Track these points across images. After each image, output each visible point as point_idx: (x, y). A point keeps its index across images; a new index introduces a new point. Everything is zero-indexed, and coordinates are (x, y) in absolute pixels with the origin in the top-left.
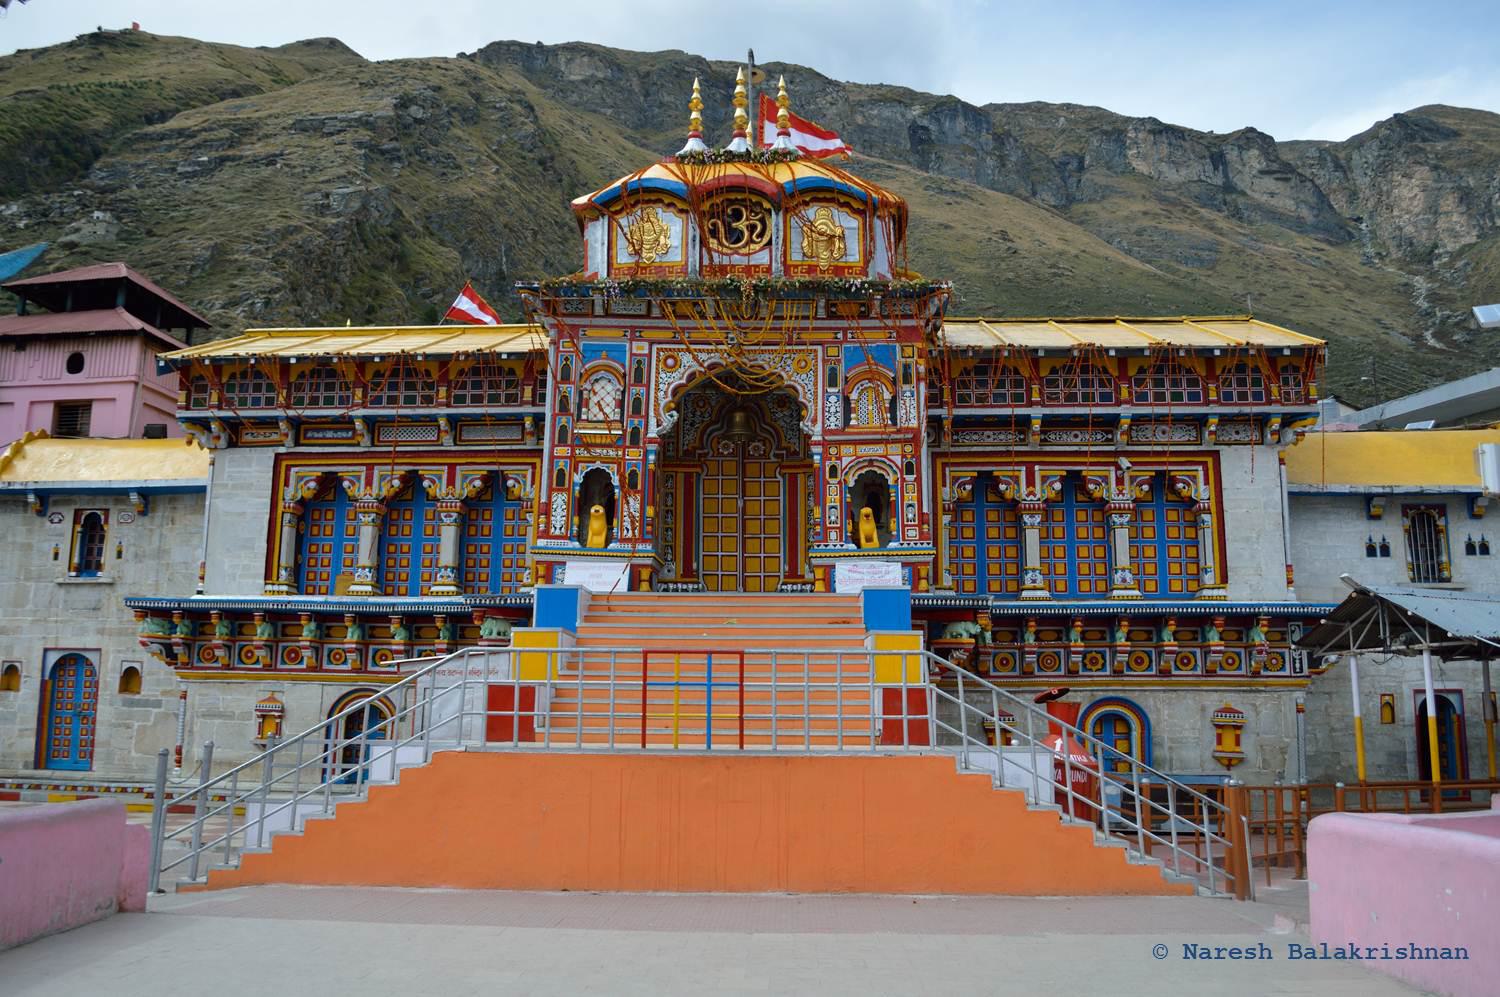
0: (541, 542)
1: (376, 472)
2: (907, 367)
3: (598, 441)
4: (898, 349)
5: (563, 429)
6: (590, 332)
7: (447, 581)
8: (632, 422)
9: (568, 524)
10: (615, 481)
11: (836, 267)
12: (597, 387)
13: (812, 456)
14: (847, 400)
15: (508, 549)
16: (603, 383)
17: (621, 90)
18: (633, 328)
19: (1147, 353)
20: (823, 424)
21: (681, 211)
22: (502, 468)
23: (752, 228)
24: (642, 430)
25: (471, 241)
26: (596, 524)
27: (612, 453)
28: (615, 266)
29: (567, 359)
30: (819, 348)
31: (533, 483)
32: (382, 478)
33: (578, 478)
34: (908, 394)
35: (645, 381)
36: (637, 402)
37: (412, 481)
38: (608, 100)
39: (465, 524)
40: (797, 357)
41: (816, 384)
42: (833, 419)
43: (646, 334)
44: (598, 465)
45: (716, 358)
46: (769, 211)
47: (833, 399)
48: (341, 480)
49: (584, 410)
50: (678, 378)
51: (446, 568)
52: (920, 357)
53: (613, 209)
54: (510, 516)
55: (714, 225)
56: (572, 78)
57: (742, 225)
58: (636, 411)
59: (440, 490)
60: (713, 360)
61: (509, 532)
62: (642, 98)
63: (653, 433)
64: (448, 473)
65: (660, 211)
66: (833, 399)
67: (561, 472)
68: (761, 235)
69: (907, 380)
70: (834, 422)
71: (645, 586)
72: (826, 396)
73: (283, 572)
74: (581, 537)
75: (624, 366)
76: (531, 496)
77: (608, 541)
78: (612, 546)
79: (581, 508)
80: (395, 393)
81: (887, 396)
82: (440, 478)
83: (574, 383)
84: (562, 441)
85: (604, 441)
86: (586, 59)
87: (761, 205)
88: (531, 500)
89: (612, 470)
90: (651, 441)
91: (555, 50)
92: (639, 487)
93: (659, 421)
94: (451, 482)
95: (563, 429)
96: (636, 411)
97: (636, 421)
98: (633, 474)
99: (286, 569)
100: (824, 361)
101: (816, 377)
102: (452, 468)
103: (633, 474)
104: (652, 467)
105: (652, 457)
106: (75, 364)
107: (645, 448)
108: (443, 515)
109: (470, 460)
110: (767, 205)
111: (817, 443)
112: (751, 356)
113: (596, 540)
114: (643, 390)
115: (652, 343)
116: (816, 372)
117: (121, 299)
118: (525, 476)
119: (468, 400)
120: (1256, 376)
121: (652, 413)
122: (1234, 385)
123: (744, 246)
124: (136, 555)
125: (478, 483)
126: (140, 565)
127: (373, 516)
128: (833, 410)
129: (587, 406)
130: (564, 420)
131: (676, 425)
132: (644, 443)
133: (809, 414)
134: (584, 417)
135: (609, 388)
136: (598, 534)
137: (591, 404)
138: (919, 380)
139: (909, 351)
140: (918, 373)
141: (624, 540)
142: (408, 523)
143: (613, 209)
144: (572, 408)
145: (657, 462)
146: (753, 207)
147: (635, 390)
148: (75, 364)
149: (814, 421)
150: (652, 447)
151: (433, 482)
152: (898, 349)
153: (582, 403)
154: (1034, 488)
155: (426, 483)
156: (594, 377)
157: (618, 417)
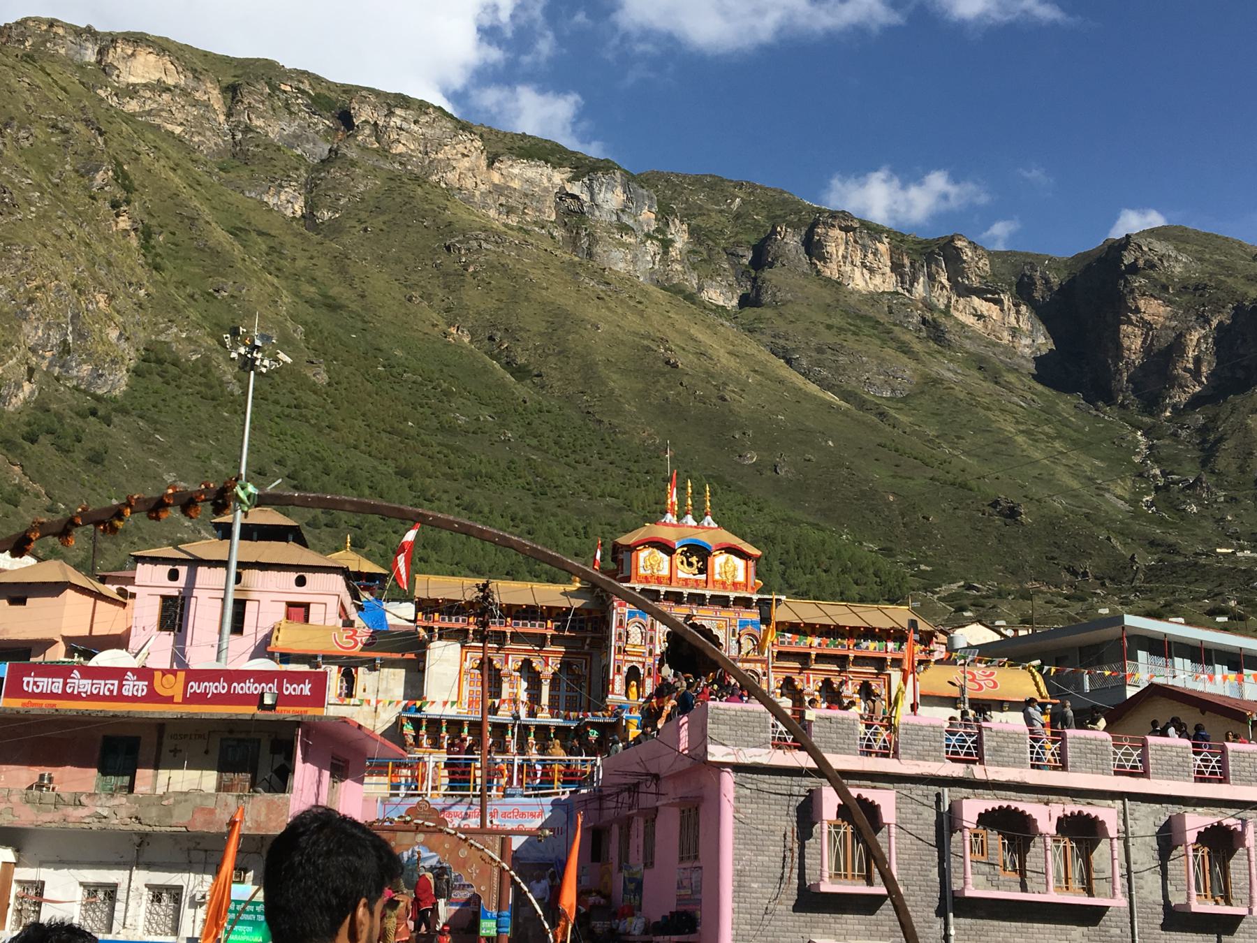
10: (642, 671)
14: (738, 642)
17: (196, 103)
25: (31, 301)
33: (625, 669)
36: (651, 638)
38: (178, 115)
56: (132, 80)
62: (222, 118)
63: (658, 651)
74: (627, 695)
84: (619, 653)
86: (152, 58)
89: (640, 666)
91: (113, 39)
106: (301, 582)
117: (291, 537)
148: (301, 582)
154: (811, 685)
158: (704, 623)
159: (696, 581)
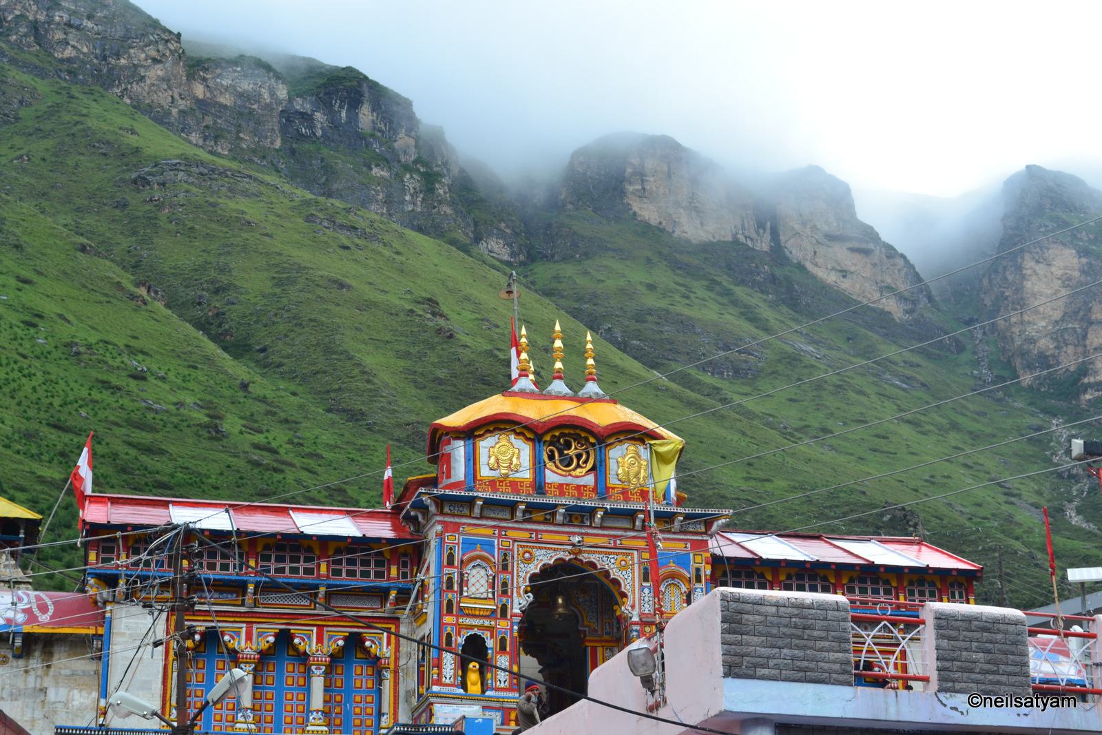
0: (435, 688)
1: (254, 631)
2: (698, 570)
3: (477, 613)
4: (691, 555)
5: (450, 603)
6: (467, 529)
7: (320, 722)
8: (501, 601)
9: (455, 676)
10: (490, 643)
11: (642, 491)
12: (474, 571)
13: (632, 631)
15: (358, 699)
16: (478, 569)
18: (500, 528)
19: (857, 568)
20: (640, 608)
21: (528, 439)
22: (361, 630)
23: (579, 456)
24: (509, 606)
26: (473, 677)
27: (487, 623)
28: (479, 478)
29: (451, 549)
30: (635, 552)
31: (389, 644)
32: (260, 634)
33: (461, 640)
34: (699, 590)
35: (510, 569)
36: (505, 584)
37: (284, 638)
39: (327, 674)
40: (620, 557)
41: (633, 579)
42: (646, 605)
43: (511, 534)
44: (475, 631)
45: (561, 555)
46: (593, 445)
47: (646, 591)
48: (223, 634)
49: (465, 589)
50: (535, 568)
51: (317, 711)
52: (707, 563)
53: (477, 433)
54: (359, 671)
55: (552, 451)
57: (572, 452)
58: (504, 593)
59: (311, 646)
60: (558, 556)
61: (358, 685)
63: (516, 611)
64: (317, 633)
65: (512, 437)
66: (646, 591)
67: (449, 636)
68: (586, 462)
69: (698, 579)
70: (648, 609)
71: (513, 723)
72: (642, 588)
73: (174, 711)
74: (464, 686)
75: (493, 556)
76: (387, 655)
77: (483, 692)
78: (488, 693)
79: (463, 666)
80: (282, 565)
81: (684, 589)
82: (309, 637)
83: (457, 568)
84: (450, 611)
85: (482, 613)
87: (587, 439)
88: (389, 658)
89: (486, 635)
90: (516, 615)
92: (508, 649)
93: (520, 602)
94: (320, 640)
95: (450, 603)
96: (504, 593)
97: (504, 600)
98: (503, 640)
99: (176, 708)
100: (640, 563)
101: (633, 573)
102: (320, 627)
103: (503, 640)
104: (516, 634)
105: (516, 628)
107: (511, 620)
108: (313, 668)
109: (336, 623)
110: (592, 440)
111: (636, 623)
112: (586, 555)
113: (475, 689)
114: (509, 576)
115: (515, 541)
116: (633, 570)
118: (380, 639)
119: (344, 575)
120: (932, 589)
121: (515, 594)
122: (917, 595)
123: (574, 470)
124: (11, 694)
125: (341, 643)
126: (19, 703)
127: (253, 666)
128: (646, 599)
129: (467, 586)
130: (450, 595)
131: (531, 604)
132: (511, 616)
133: (629, 602)
134: (465, 594)
135: (483, 572)
136: (474, 684)
137: (470, 584)
138: (706, 580)
139: (698, 559)
140: (706, 575)
141: (497, 689)
142: (271, 674)
143: (477, 433)
144: (456, 587)
145: (520, 630)
146: (578, 438)
147: (501, 576)
149: (633, 607)
150: (517, 619)
151: (304, 640)
152: (691, 555)
153: (462, 583)
155: (296, 641)
156: (472, 564)
157: (490, 595)
158: (594, 558)
159: (578, 487)
